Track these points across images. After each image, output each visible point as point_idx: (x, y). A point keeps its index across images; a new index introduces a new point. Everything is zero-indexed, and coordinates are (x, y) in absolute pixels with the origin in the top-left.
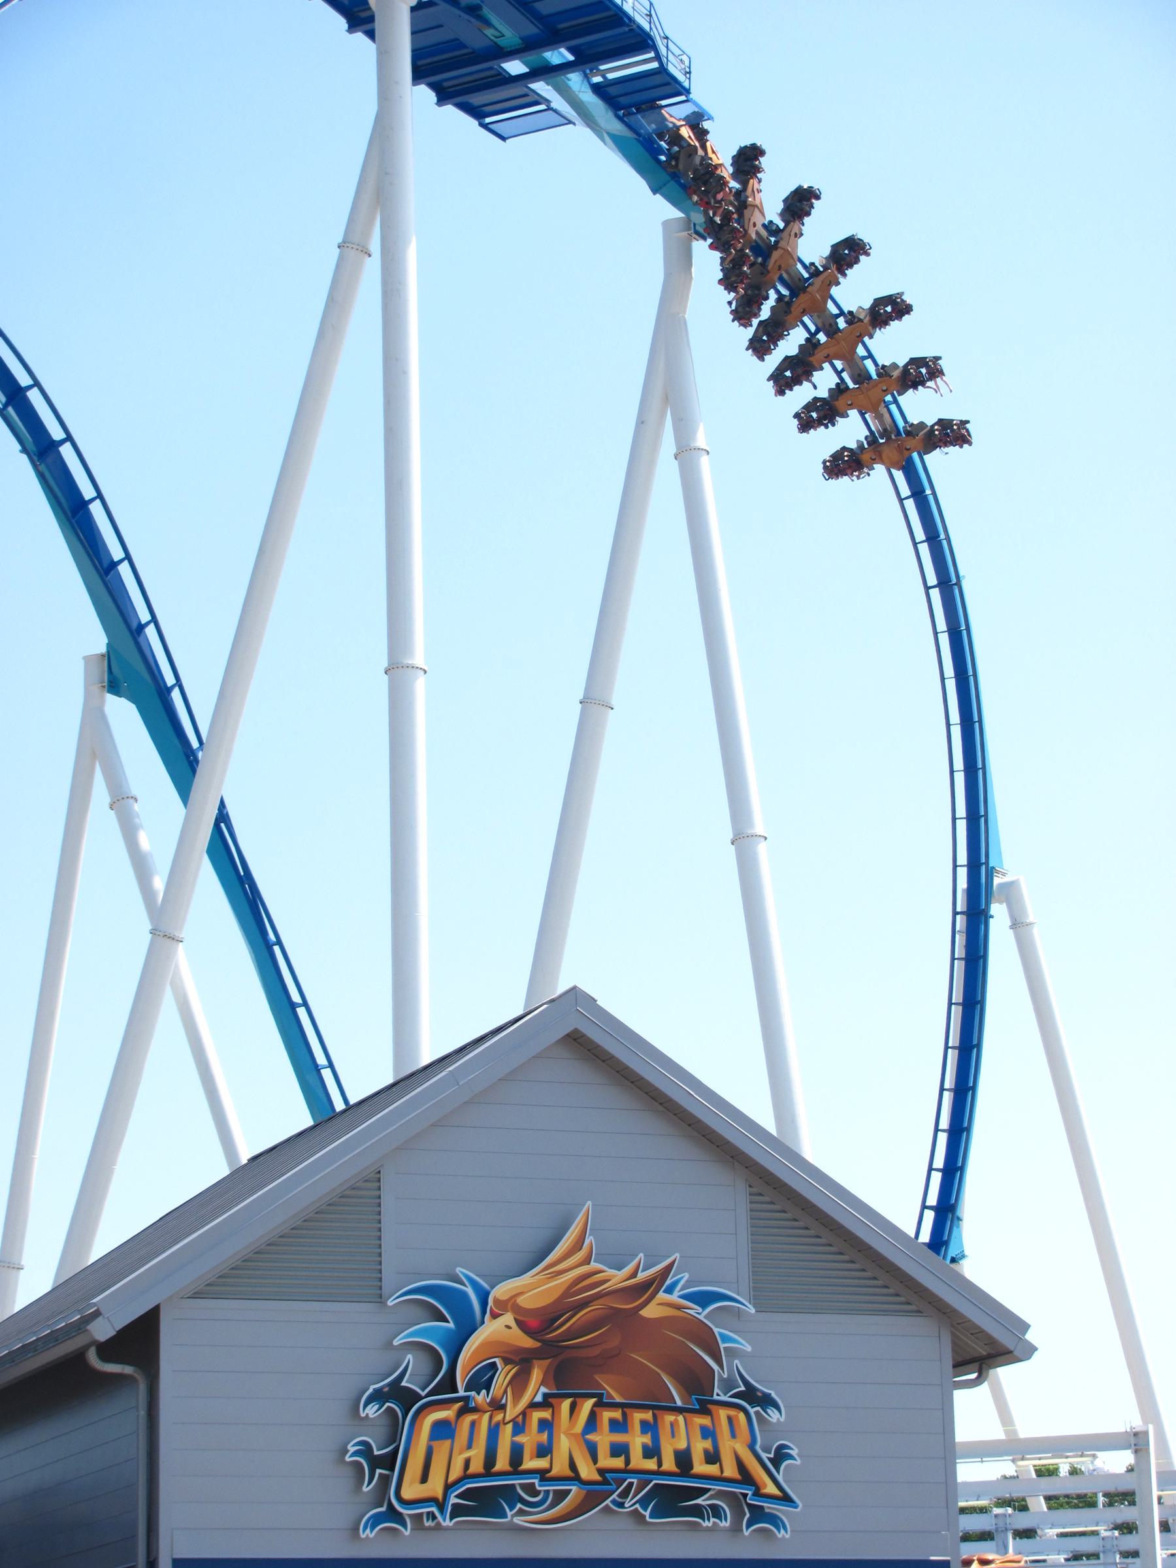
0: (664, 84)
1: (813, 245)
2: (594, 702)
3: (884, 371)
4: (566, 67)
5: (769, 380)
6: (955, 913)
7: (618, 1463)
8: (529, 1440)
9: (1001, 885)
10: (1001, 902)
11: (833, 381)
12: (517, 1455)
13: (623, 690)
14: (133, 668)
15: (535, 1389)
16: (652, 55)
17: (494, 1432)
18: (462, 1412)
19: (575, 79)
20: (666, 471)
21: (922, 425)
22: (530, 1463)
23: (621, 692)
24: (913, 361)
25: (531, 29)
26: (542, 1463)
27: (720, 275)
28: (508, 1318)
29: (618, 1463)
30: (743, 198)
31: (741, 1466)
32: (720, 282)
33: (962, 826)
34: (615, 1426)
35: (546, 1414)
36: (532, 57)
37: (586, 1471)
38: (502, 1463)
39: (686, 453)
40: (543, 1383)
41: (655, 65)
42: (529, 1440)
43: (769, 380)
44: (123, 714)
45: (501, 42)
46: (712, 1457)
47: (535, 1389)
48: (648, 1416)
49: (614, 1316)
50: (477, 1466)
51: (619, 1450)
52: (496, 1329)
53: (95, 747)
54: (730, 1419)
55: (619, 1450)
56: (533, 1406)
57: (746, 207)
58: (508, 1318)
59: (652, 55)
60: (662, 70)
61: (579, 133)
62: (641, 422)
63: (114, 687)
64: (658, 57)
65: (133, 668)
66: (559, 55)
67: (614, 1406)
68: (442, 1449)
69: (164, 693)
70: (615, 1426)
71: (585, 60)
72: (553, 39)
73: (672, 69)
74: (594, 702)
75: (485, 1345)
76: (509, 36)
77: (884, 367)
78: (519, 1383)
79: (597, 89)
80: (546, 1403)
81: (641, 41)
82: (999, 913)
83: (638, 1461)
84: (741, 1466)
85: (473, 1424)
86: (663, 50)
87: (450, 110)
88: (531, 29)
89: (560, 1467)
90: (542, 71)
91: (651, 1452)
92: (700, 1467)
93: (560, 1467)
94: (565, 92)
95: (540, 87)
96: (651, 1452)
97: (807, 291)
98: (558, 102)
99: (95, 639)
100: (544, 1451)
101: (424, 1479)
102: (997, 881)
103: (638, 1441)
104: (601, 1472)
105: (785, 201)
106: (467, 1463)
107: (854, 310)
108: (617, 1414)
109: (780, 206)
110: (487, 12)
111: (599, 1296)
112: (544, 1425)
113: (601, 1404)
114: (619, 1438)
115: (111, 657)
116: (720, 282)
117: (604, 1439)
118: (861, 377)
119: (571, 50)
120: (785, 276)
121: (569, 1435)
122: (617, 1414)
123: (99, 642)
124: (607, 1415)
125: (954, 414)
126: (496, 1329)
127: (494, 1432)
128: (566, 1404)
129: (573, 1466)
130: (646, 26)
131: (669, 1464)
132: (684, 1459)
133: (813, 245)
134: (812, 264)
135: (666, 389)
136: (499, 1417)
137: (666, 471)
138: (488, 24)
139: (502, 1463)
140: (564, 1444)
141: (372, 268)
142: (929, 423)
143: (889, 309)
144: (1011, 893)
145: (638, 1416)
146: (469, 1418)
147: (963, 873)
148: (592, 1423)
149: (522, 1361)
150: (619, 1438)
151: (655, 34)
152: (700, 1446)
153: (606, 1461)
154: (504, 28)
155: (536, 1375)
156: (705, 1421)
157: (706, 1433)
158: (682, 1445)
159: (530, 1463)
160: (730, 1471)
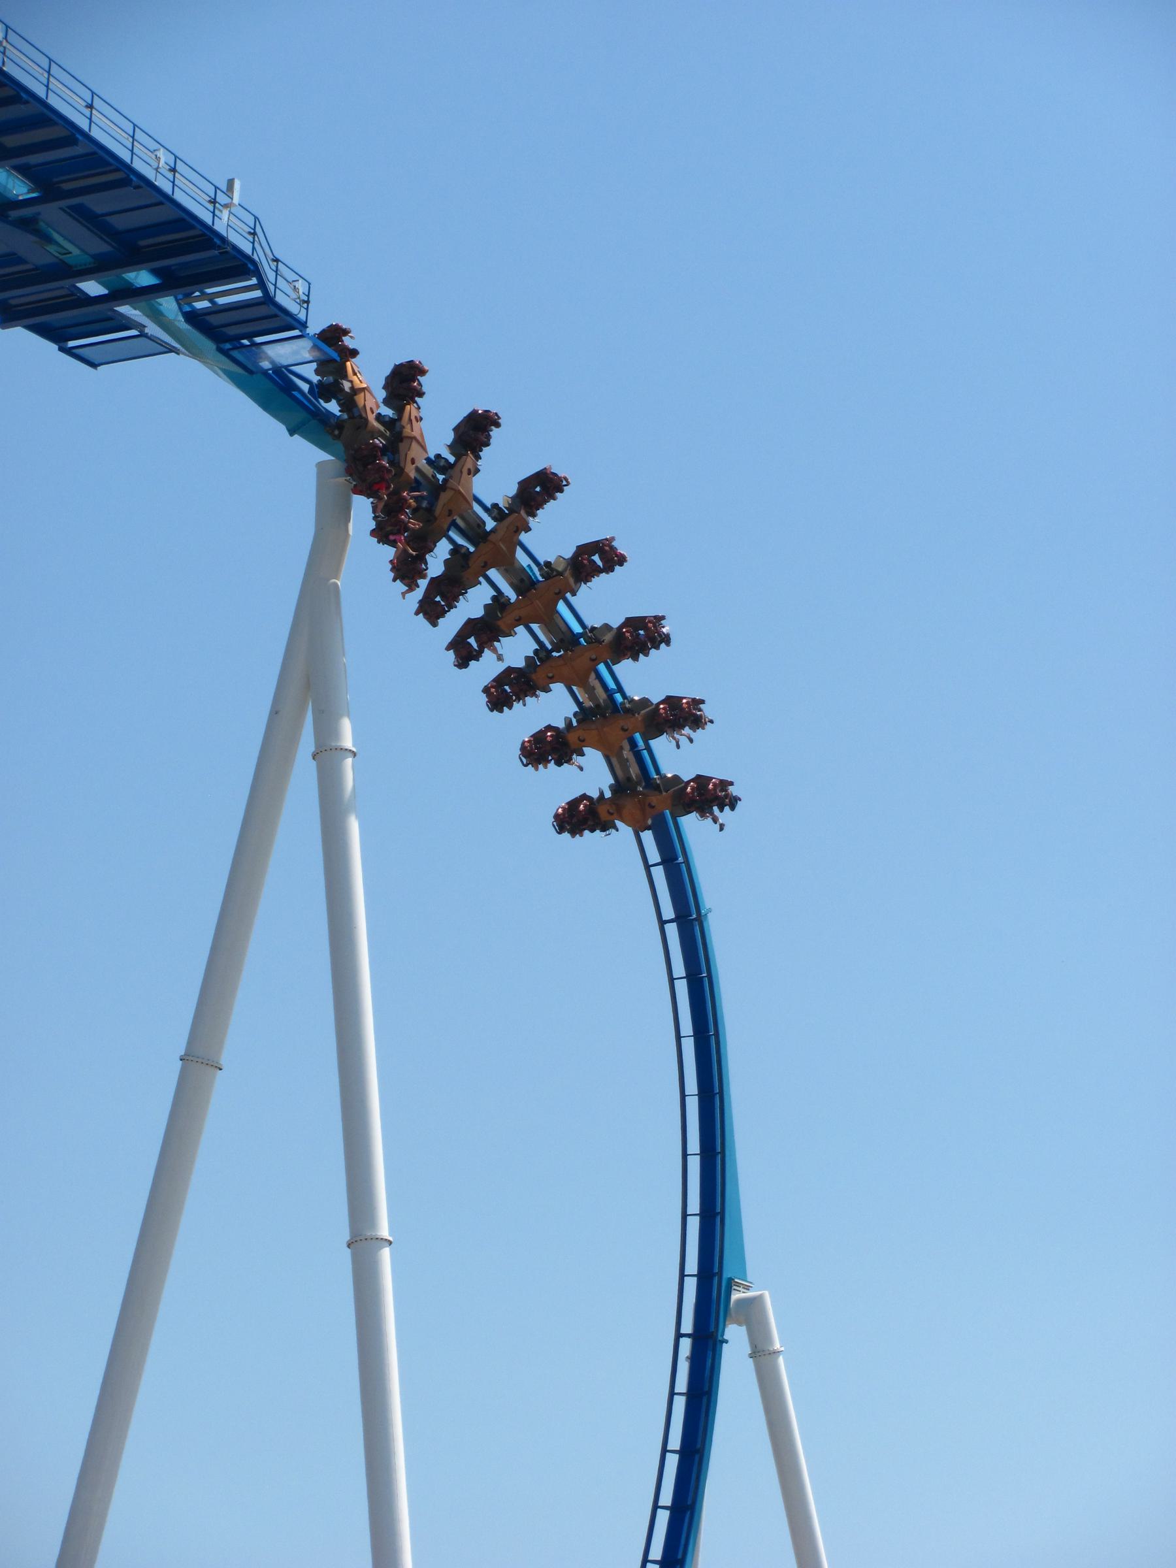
1: (494, 480)
2: (199, 1060)
5: (448, 649)
6: (679, 1335)
9: (740, 1302)
10: (740, 1324)
11: (530, 647)
13: (236, 1046)
16: (254, 281)
19: (168, 304)
20: (303, 774)
21: (645, 702)
27: (373, 525)
30: (397, 429)
32: (373, 533)
36: (110, 276)
41: (258, 294)
43: (448, 649)
57: (401, 441)
59: (254, 281)
60: (269, 299)
64: (262, 285)
66: (143, 278)
72: (134, 257)
73: (280, 299)
74: (199, 1060)
76: (75, 254)
77: (593, 629)
79: (192, 317)
81: (239, 266)
82: (735, 1338)
86: (271, 275)
94: (157, 316)
97: (492, 541)
102: (735, 1296)
105: (456, 429)
107: (552, 559)
109: (450, 437)
116: (373, 533)
119: (155, 272)
120: (459, 522)
125: (685, 690)
130: (246, 247)
133: (494, 480)
134: (495, 506)
137: (303, 774)
138: (49, 240)
142: (655, 701)
143: (597, 558)
144: (752, 1314)
151: (260, 257)
154: (70, 242)
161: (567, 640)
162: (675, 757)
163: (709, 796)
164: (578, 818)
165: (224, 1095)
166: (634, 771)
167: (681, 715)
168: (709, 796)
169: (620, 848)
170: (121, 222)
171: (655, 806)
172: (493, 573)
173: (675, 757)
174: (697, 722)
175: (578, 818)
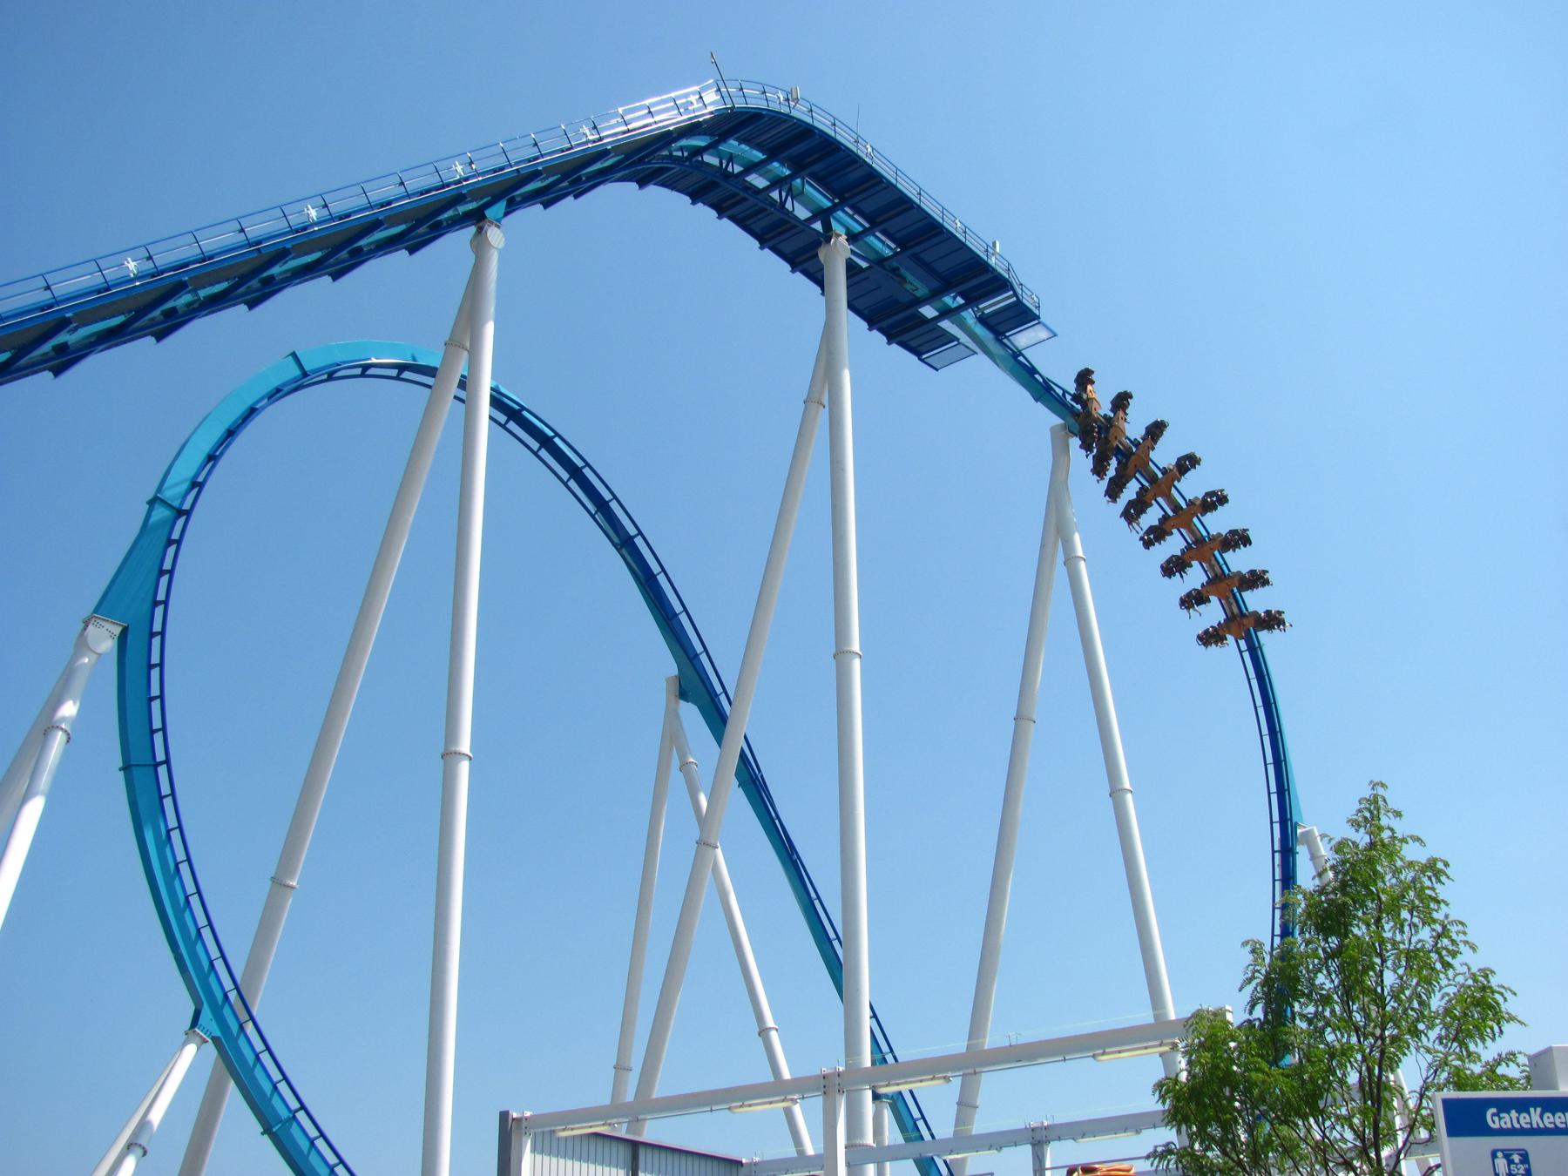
0: (1022, 315)
3: (1190, 503)
4: (960, 308)
14: (697, 686)
19: (969, 316)
20: (1060, 572)
23: (1037, 710)
24: (1207, 494)
25: (936, 284)
33: (1274, 798)
36: (938, 304)
39: (1070, 561)
44: (690, 714)
45: (919, 294)
53: (673, 738)
60: (1019, 303)
61: (981, 360)
62: (1043, 546)
63: (683, 695)
64: (1015, 294)
65: (697, 686)
69: (713, 696)
71: (971, 300)
76: (922, 291)
79: (983, 320)
81: (1000, 284)
87: (895, 346)
88: (936, 284)
90: (946, 313)
95: (945, 324)
98: (964, 338)
99: (669, 666)
110: (903, 271)
115: (680, 679)
118: (1176, 508)
123: (672, 669)
135: (1056, 529)
141: (824, 414)
144: (1308, 838)
147: (1277, 827)
161: (1199, 541)
162: (1256, 601)
163: (1272, 621)
164: (1210, 638)
165: (1035, 735)
166: (1236, 610)
167: (1257, 579)
168: (1272, 621)
169: (1230, 652)
170: (941, 267)
171: (1246, 628)
172: (1160, 499)
173: (1256, 601)
174: (1266, 582)
175: (1210, 638)
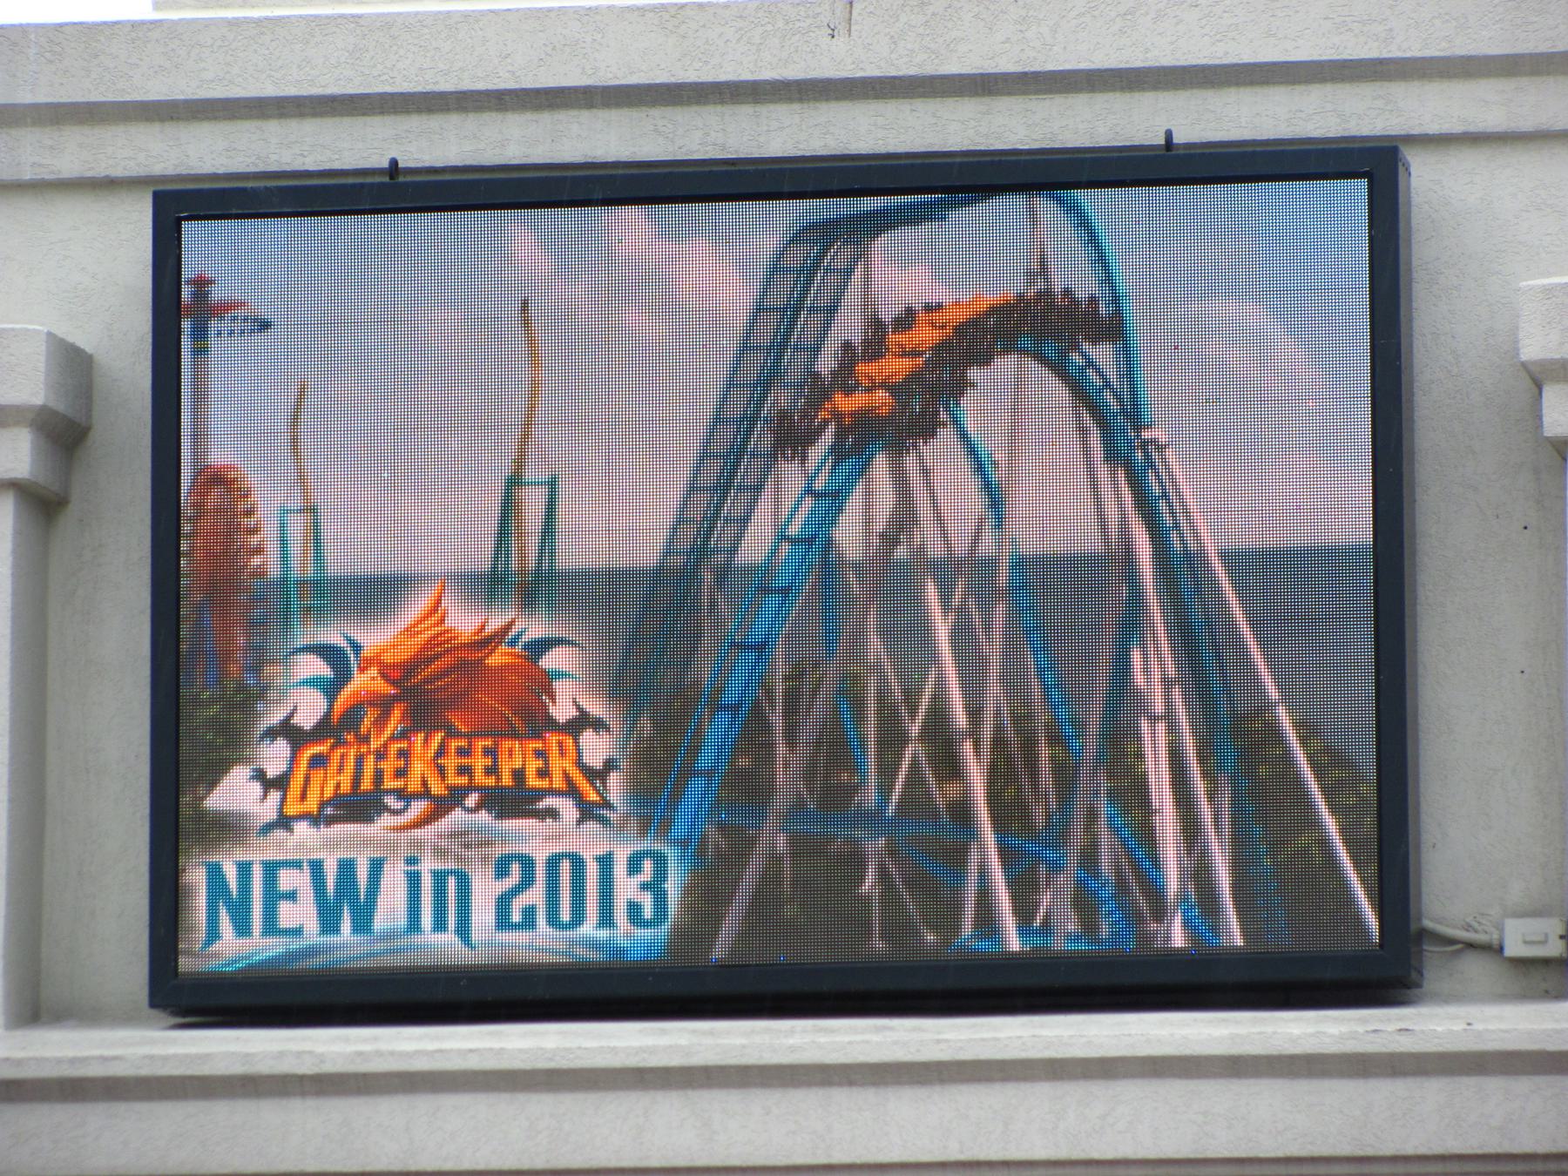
7: (463, 780)
8: (388, 766)
12: (378, 776)
15: (394, 724)
17: (360, 761)
18: (333, 747)
22: (389, 784)
26: (398, 784)
28: (373, 672)
29: (463, 780)
31: (567, 777)
34: (461, 752)
35: (404, 745)
37: (436, 788)
38: (366, 784)
40: (402, 720)
42: (388, 766)
46: (543, 773)
47: (394, 724)
48: (489, 743)
49: (461, 666)
50: (346, 787)
51: (464, 770)
52: (363, 682)
54: (560, 744)
55: (464, 770)
56: (392, 739)
58: (373, 672)
67: (459, 735)
68: (317, 777)
70: (461, 752)
75: (356, 694)
78: (381, 722)
80: (404, 735)
83: (480, 778)
84: (567, 777)
85: (342, 756)
89: (414, 785)
91: (492, 770)
92: (533, 782)
93: (414, 785)
96: (492, 770)
100: (401, 773)
101: (303, 797)
103: (479, 763)
104: (449, 788)
106: (338, 786)
108: (463, 743)
111: (448, 651)
112: (402, 754)
113: (451, 733)
114: (465, 761)
117: (451, 762)
121: (422, 758)
122: (463, 743)
124: (454, 744)
126: (363, 682)
127: (360, 761)
128: (420, 737)
129: (424, 783)
131: (507, 780)
132: (519, 775)
136: (364, 749)
139: (366, 784)
140: (417, 768)
145: (480, 744)
146: (339, 752)
148: (442, 751)
149: (384, 705)
150: (465, 761)
152: (533, 765)
153: (454, 780)
155: (397, 713)
156: (539, 745)
157: (539, 754)
158: (518, 764)
159: (389, 784)
160: (558, 783)
